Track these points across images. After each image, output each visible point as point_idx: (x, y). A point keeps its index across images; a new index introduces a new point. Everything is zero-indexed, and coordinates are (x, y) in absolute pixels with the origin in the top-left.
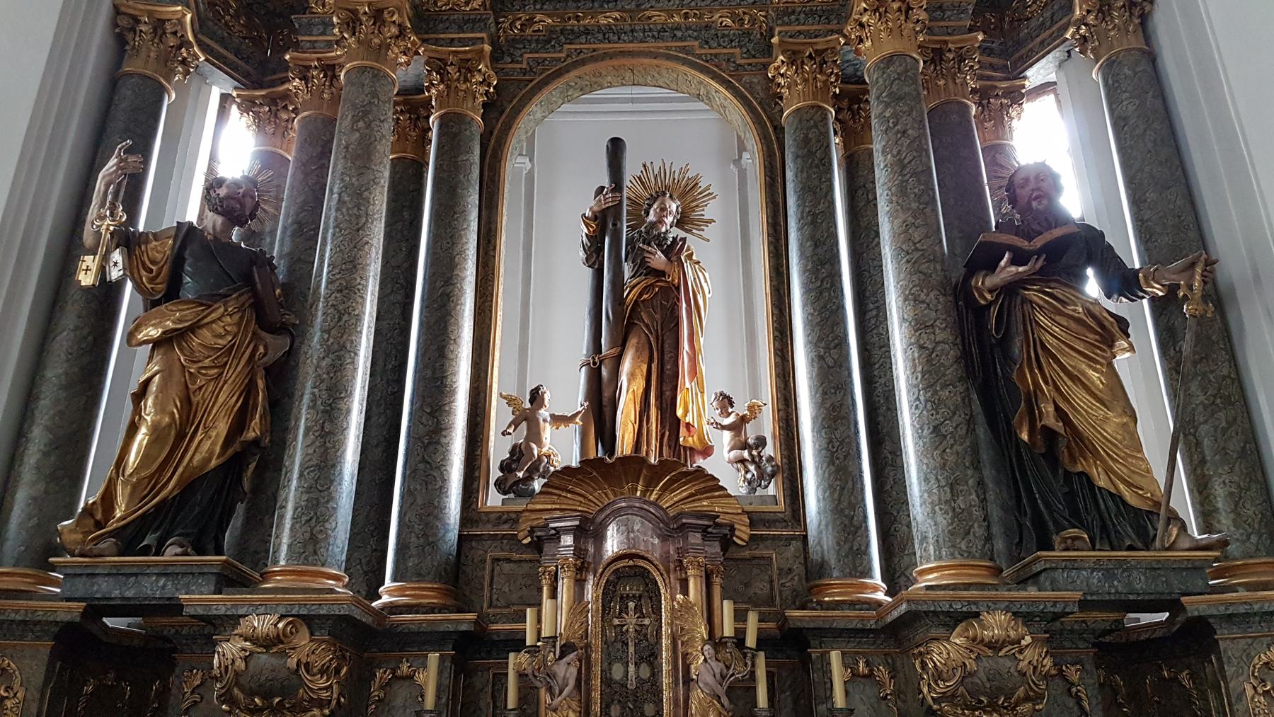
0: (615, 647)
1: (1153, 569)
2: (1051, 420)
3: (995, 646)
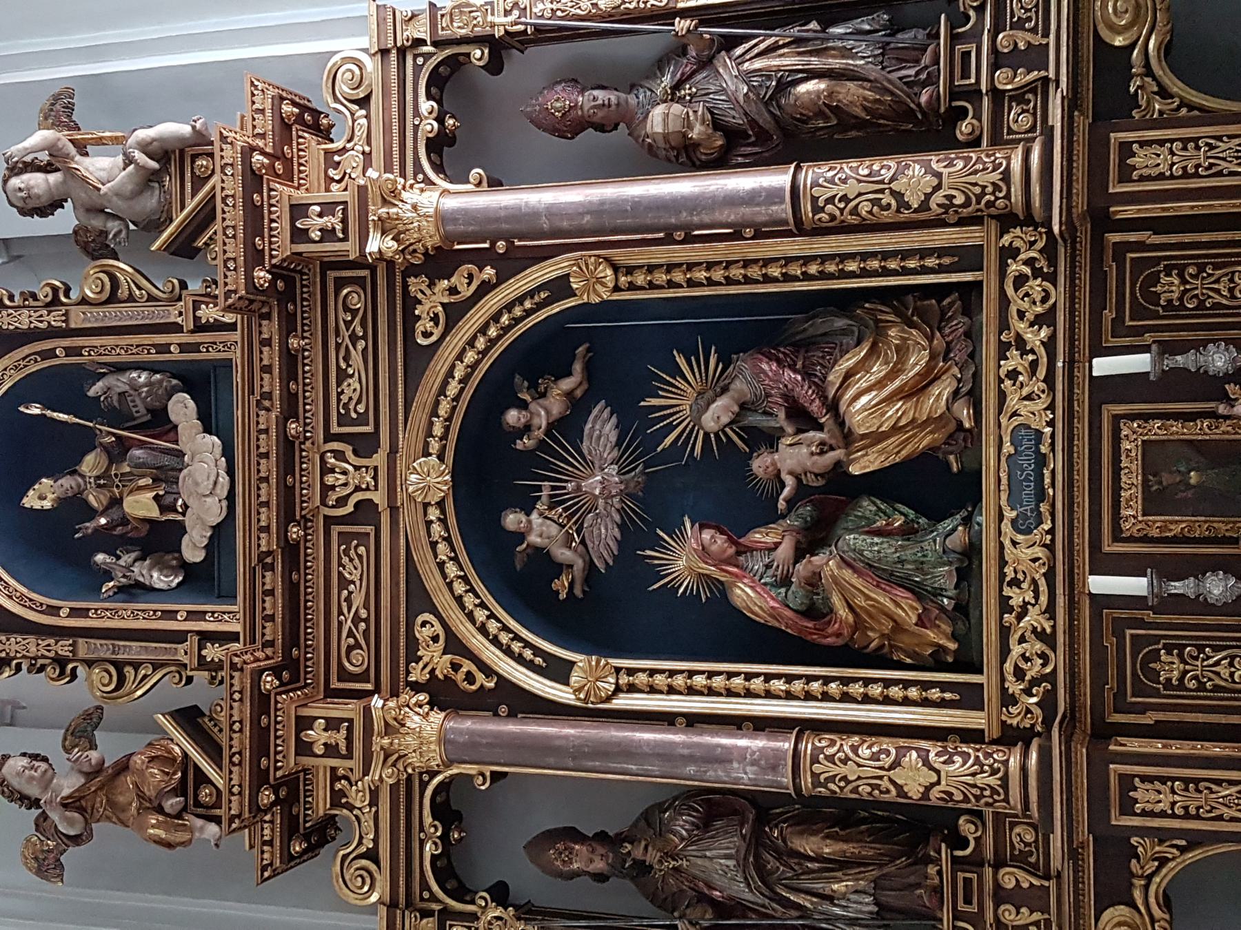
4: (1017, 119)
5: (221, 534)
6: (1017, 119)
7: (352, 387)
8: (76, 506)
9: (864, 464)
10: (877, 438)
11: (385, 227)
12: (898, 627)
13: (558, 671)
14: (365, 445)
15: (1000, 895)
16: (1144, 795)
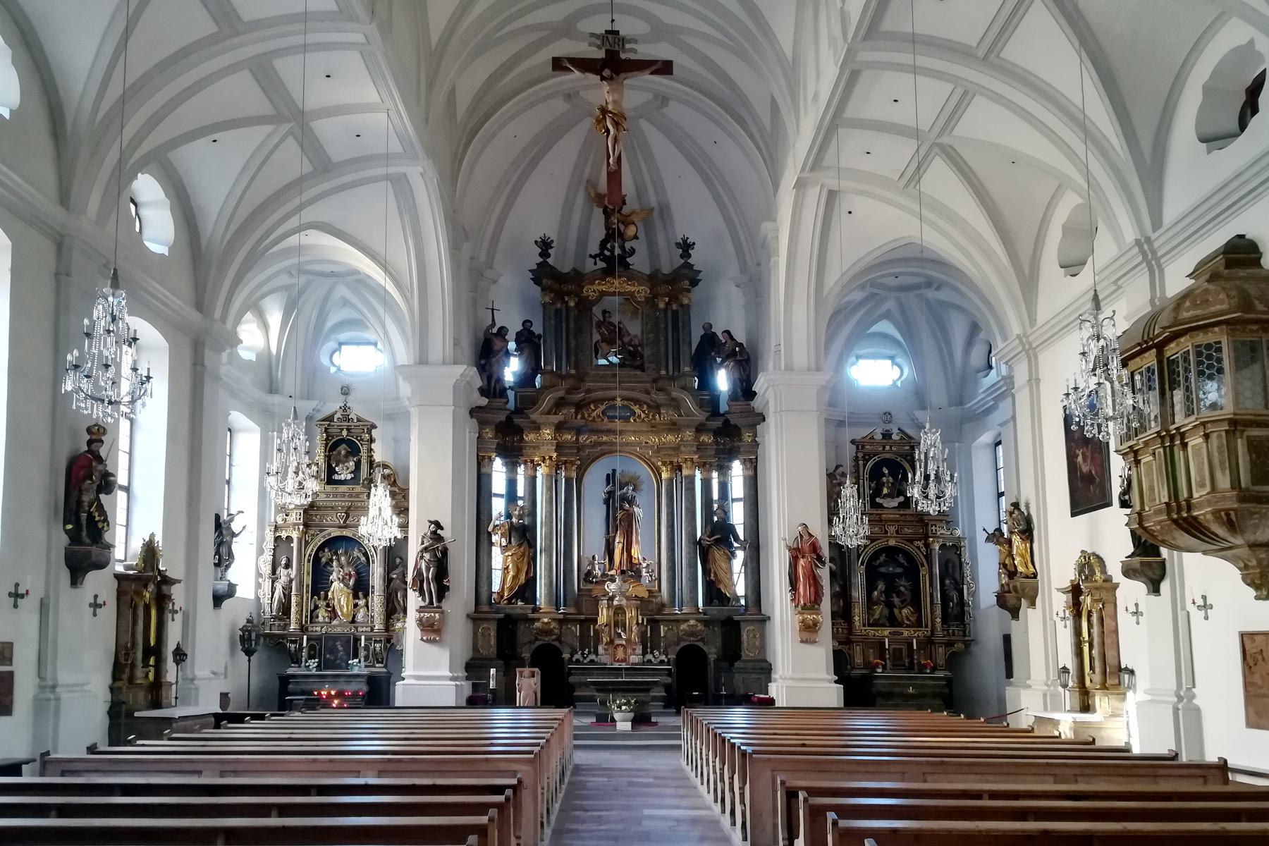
0: (616, 625)
1: (728, 610)
2: (712, 578)
3: (692, 626)
4: (945, 633)
5: (880, 506)
6: (945, 633)
7: (906, 530)
8: (884, 475)
9: (896, 611)
10: (901, 613)
11: (933, 542)
12: (873, 615)
13: (862, 564)
14: (897, 532)
15: (838, 629)
16: (858, 647)
